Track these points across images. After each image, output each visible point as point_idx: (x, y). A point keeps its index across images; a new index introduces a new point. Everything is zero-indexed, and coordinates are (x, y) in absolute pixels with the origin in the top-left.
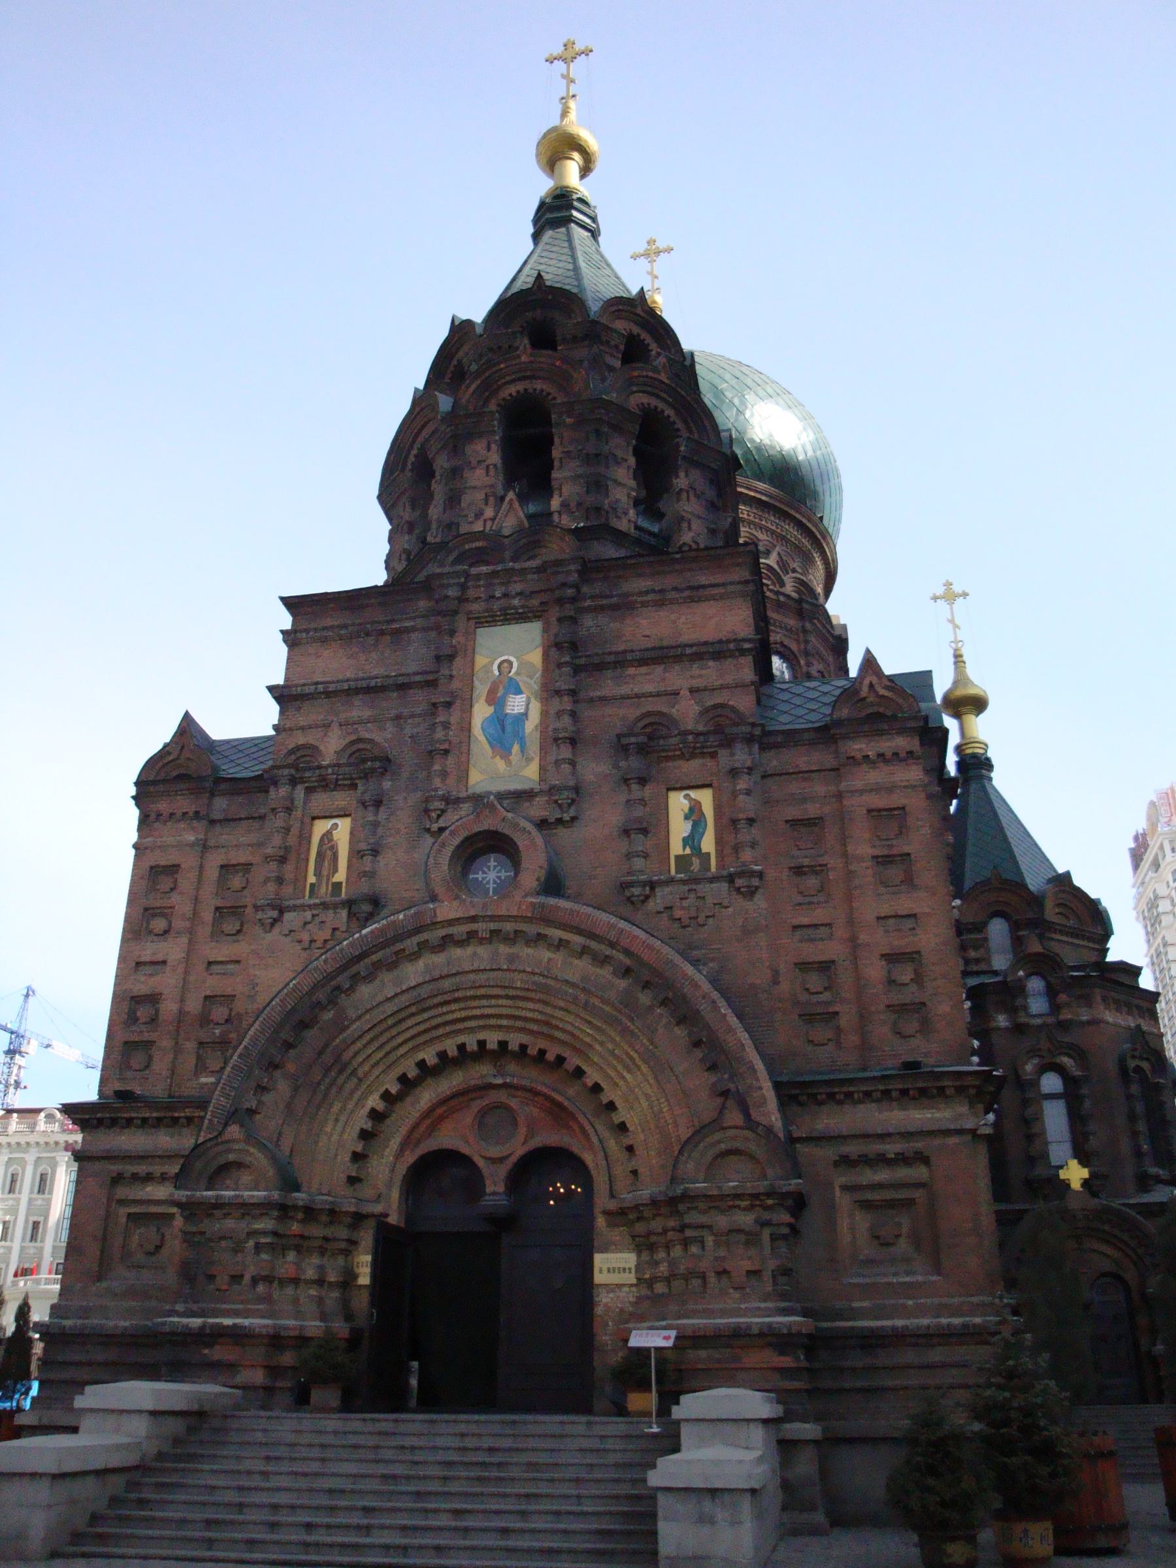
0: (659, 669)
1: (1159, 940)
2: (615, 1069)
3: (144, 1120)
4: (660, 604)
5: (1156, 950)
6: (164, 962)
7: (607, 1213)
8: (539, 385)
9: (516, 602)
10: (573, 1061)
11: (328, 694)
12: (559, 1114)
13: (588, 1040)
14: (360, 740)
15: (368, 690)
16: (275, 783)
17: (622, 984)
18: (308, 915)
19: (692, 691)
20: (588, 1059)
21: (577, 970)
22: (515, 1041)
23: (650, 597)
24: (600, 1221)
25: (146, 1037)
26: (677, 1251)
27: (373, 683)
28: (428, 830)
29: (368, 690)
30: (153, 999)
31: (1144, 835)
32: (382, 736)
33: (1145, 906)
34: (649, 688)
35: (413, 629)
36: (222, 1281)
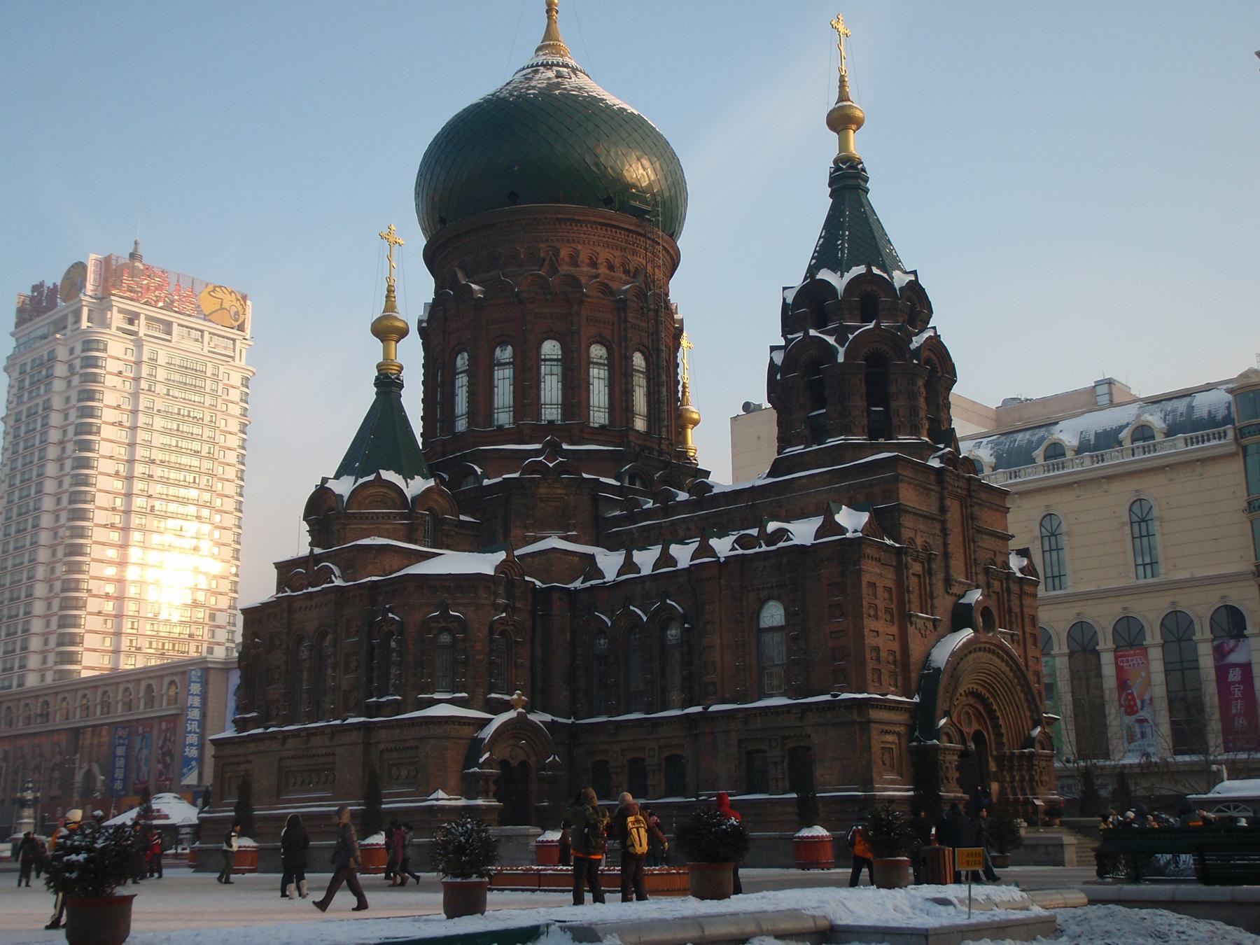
0: (990, 538)
1: (40, 401)
2: (1003, 705)
3: (890, 707)
4: (990, 508)
5: (29, 409)
6: (877, 632)
7: (991, 756)
8: (934, 358)
9: (959, 491)
10: (991, 700)
11: (915, 514)
12: (979, 716)
13: (999, 693)
14: (925, 541)
15: (926, 517)
16: (906, 554)
17: (1012, 674)
18: (922, 621)
19: (1000, 552)
20: (996, 701)
21: (1003, 666)
22: (980, 689)
23: (988, 504)
24: (990, 759)
25: (878, 667)
26: (1024, 773)
27: (928, 514)
28: (948, 593)
29: (926, 517)
30: (877, 649)
31: (54, 291)
32: (931, 541)
33: (29, 361)
34: (989, 546)
35: (933, 490)
36: (950, 779)
